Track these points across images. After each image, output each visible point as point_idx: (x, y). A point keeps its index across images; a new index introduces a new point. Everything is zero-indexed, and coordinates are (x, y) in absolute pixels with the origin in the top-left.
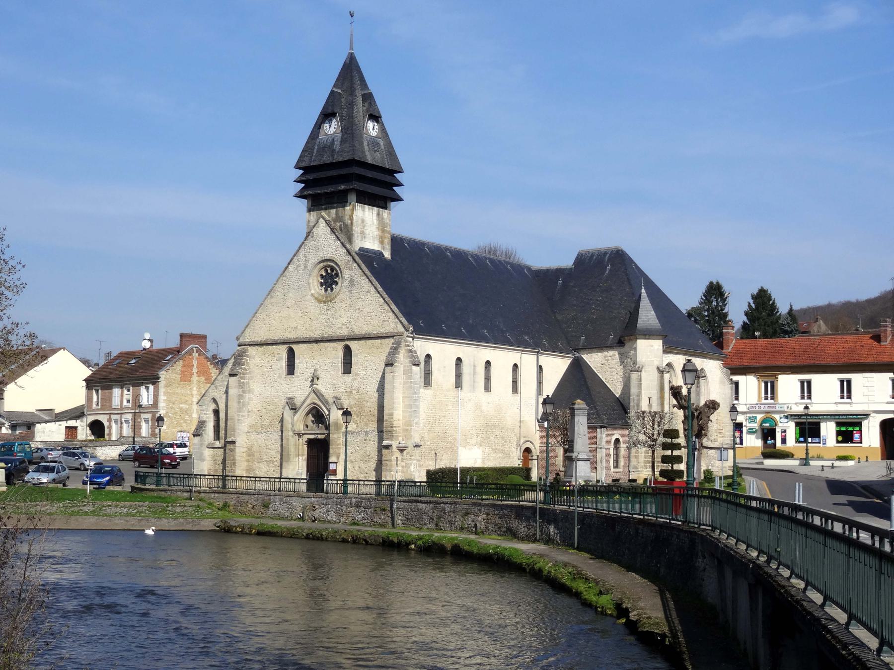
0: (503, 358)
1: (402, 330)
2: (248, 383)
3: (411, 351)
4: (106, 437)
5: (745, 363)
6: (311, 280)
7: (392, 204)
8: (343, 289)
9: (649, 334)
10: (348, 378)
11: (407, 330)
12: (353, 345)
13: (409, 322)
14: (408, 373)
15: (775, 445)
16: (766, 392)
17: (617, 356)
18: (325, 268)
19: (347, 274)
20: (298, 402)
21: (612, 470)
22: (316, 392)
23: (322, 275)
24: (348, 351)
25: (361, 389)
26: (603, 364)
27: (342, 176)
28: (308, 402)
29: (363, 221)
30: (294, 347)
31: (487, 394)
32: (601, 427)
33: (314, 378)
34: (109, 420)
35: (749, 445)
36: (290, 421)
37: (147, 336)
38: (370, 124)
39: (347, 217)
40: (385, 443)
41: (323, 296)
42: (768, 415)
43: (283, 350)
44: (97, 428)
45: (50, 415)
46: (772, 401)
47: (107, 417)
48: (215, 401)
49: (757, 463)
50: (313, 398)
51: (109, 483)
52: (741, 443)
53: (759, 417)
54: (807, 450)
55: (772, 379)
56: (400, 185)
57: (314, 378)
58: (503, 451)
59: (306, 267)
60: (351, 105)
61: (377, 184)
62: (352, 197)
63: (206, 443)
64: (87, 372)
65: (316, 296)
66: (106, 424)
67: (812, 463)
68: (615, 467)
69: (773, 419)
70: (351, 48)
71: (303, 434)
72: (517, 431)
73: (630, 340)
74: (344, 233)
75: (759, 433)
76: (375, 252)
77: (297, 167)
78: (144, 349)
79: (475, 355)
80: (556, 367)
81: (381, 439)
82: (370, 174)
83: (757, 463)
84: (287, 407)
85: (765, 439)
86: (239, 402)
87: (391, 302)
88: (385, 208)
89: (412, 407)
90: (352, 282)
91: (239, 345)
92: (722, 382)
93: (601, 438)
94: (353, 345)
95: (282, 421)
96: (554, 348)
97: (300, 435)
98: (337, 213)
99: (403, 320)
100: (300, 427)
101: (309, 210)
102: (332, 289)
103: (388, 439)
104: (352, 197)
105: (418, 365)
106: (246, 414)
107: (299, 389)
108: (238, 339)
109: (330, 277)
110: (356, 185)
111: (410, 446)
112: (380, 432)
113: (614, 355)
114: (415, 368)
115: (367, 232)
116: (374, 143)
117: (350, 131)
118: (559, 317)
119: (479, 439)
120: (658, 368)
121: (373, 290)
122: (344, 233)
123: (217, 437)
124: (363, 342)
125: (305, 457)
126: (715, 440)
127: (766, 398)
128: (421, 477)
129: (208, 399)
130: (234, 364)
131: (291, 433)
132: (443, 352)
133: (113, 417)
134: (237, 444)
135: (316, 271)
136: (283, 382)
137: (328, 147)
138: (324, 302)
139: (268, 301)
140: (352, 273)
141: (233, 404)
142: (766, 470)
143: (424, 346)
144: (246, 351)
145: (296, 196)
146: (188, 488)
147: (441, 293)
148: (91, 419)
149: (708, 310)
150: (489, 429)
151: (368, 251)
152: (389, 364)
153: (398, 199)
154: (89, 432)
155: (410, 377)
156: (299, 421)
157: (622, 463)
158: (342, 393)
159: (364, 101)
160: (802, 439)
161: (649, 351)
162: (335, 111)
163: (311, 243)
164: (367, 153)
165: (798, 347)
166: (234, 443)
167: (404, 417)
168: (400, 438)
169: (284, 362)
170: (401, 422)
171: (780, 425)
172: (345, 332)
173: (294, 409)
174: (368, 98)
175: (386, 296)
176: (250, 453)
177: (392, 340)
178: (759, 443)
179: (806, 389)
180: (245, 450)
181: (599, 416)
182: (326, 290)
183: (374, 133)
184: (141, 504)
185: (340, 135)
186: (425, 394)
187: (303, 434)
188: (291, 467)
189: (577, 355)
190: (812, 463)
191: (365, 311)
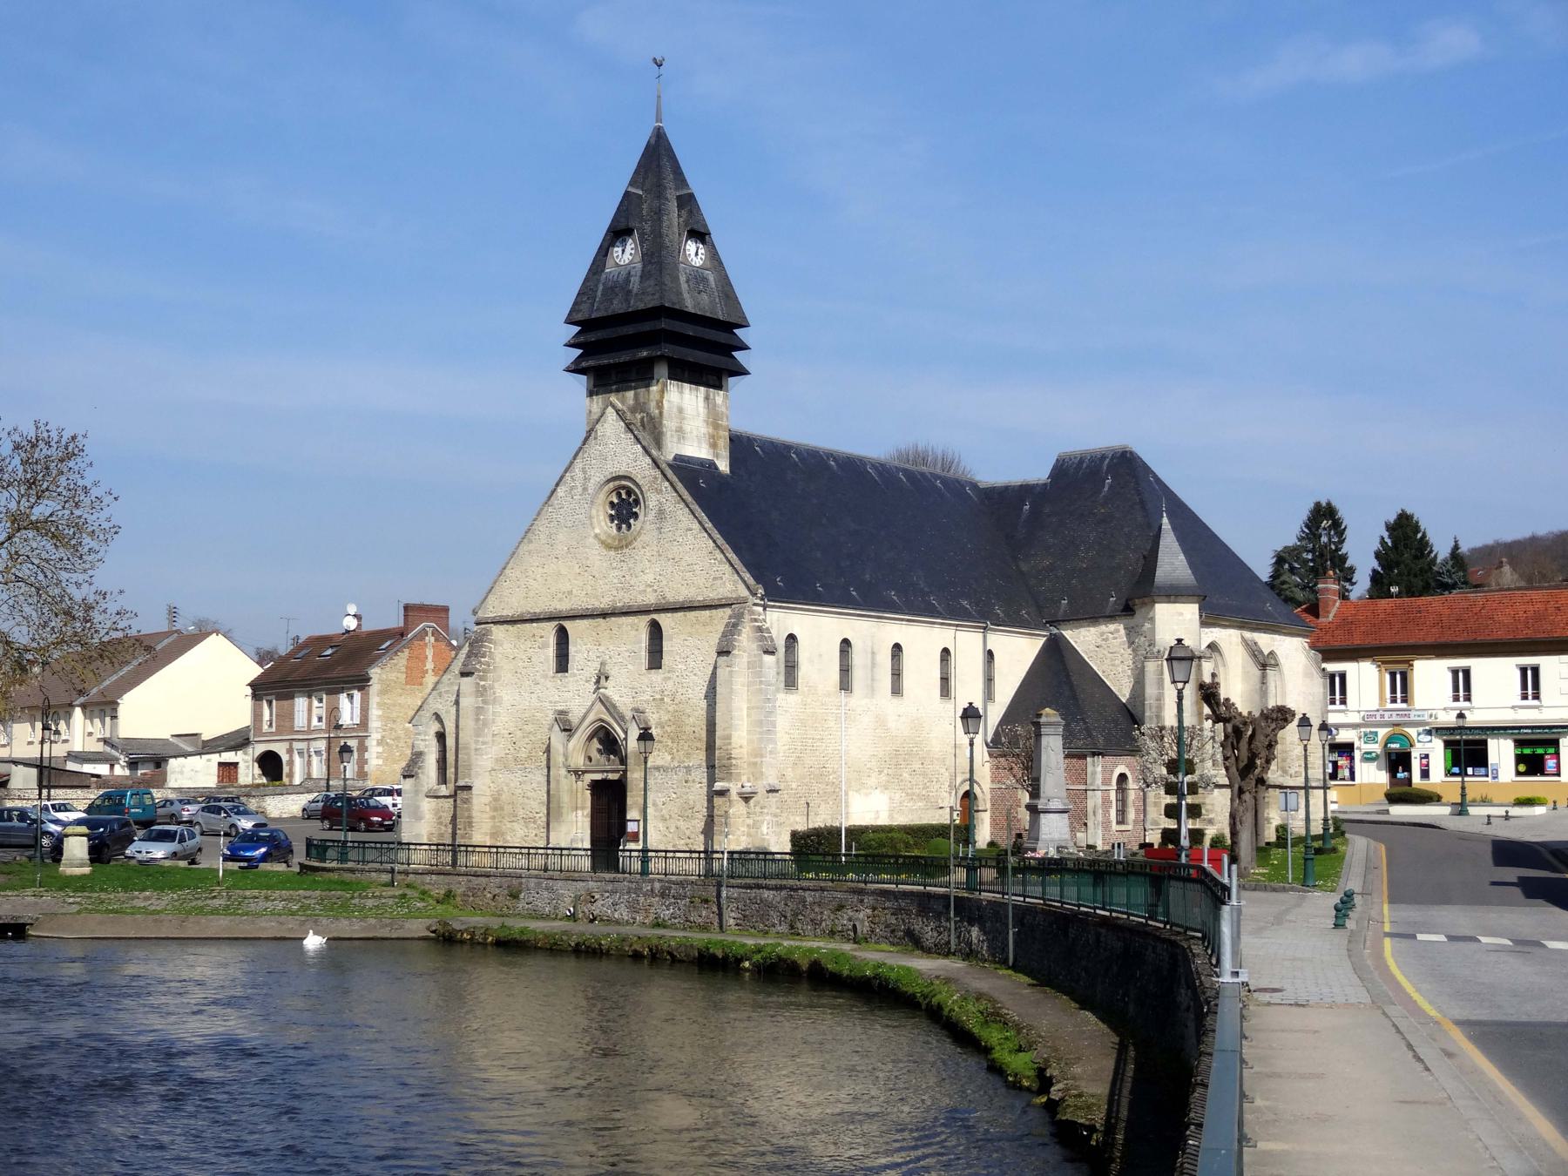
0: (922, 639)
1: (746, 593)
2: (492, 687)
3: (760, 629)
4: (285, 780)
5: (1357, 641)
6: (594, 512)
7: (731, 380)
8: (648, 526)
9: (1175, 594)
10: (656, 676)
11: (754, 595)
12: (664, 620)
13: (758, 579)
14: (755, 667)
15: (1409, 781)
16: (1393, 690)
17: (1123, 632)
18: (617, 490)
19: (652, 500)
20: (574, 718)
21: (1115, 827)
22: (604, 701)
23: (612, 503)
24: (656, 631)
25: (679, 696)
26: (1100, 646)
27: (645, 334)
28: (591, 717)
29: (681, 410)
30: (567, 624)
31: (896, 700)
32: (1094, 754)
33: (601, 677)
34: (290, 751)
35: (1365, 781)
36: (561, 750)
37: (352, 609)
38: (691, 247)
39: (653, 404)
40: (718, 786)
41: (614, 538)
42: (1397, 730)
43: (549, 631)
44: (271, 765)
45: (192, 744)
46: (1404, 706)
47: (286, 745)
48: (438, 717)
49: (1379, 812)
50: (599, 712)
51: (265, 858)
52: (1352, 777)
53: (1383, 732)
54: (1463, 788)
55: (1403, 667)
56: (744, 347)
57: (601, 677)
58: (926, 798)
59: (585, 489)
60: (658, 213)
61: (706, 347)
62: (662, 370)
63: (425, 789)
64: (255, 671)
65: (603, 537)
66: (285, 758)
67: (1472, 810)
68: (1118, 823)
69: (1407, 737)
70: (659, 119)
71: (584, 772)
72: (950, 761)
73: (1144, 604)
74: (648, 430)
75: (1383, 760)
76: (701, 462)
77: (570, 321)
78: (348, 631)
79: (873, 634)
80: (1018, 652)
81: (712, 780)
82: (690, 330)
83: (1379, 812)
84: (556, 728)
85: (1393, 771)
86: (478, 720)
87: (726, 547)
88: (719, 387)
89: (764, 725)
90: (661, 513)
91: (478, 624)
92: (1307, 675)
93: (1094, 773)
94: (664, 620)
95: (548, 750)
96: (1014, 621)
97: (578, 773)
98: (636, 397)
99: (747, 576)
100: (579, 761)
101: (591, 394)
102: (629, 527)
103: (722, 779)
104: (662, 370)
105: (772, 653)
106: (489, 739)
107: (575, 695)
108: (475, 612)
109: (625, 507)
110: (667, 350)
111: (762, 791)
112: (711, 767)
113: (1117, 631)
114: (768, 658)
115: (687, 428)
116: (697, 278)
117: (657, 258)
118: (1024, 567)
119: (883, 778)
121: (696, 526)
122: (648, 430)
123: (443, 779)
124: (680, 614)
125: (588, 811)
127: (1394, 701)
128: (780, 843)
129: (427, 714)
130: (468, 656)
131: (563, 772)
132: (817, 630)
133: (296, 745)
134: (474, 791)
135: (602, 496)
136: (549, 684)
137: (620, 287)
138: (616, 549)
139: (524, 547)
140: (661, 497)
141: (467, 723)
142: (1393, 823)
143: (782, 620)
144: (488, 632)
145: (568, 370)
146: (388, 866)
147: (816, 530)
148: (260, 749)
149: (1312, 551)
150: (900, 761)
151: (689, 460)
152: (723, 652)
153: (741, 371)
154: (257, 771)
155: (759, 674)
156: (576, 751)
157: (1131, 815)
158: (647, 702)
159: (680, 207)
160: (1456, 770)
161: (1175, 621)
162: (632, 224)
163: (593, 448)
164: (686, 295)
165: (1447, 612)
166: (469, 788)
167: (750, 741)
168: (744, 778)
169: (551, 651)
170: (744, 751)
171: (1418, 745)
172: (650, 599)
173: (568, 730)
174: (688, 202)
175: (717, 536)
176: (496, 805)
177: (728, 611)
178: (1381, 777)
179: (1463, 684)
180: (487, 800)
181: (1090, 735)
182: (619, 528)
183: (697, 262)
184: (308, 893)
185: (639, 266)
186: (787, 702)
187: (584, 772)
188: (564, 828)
190: (1472, 810)
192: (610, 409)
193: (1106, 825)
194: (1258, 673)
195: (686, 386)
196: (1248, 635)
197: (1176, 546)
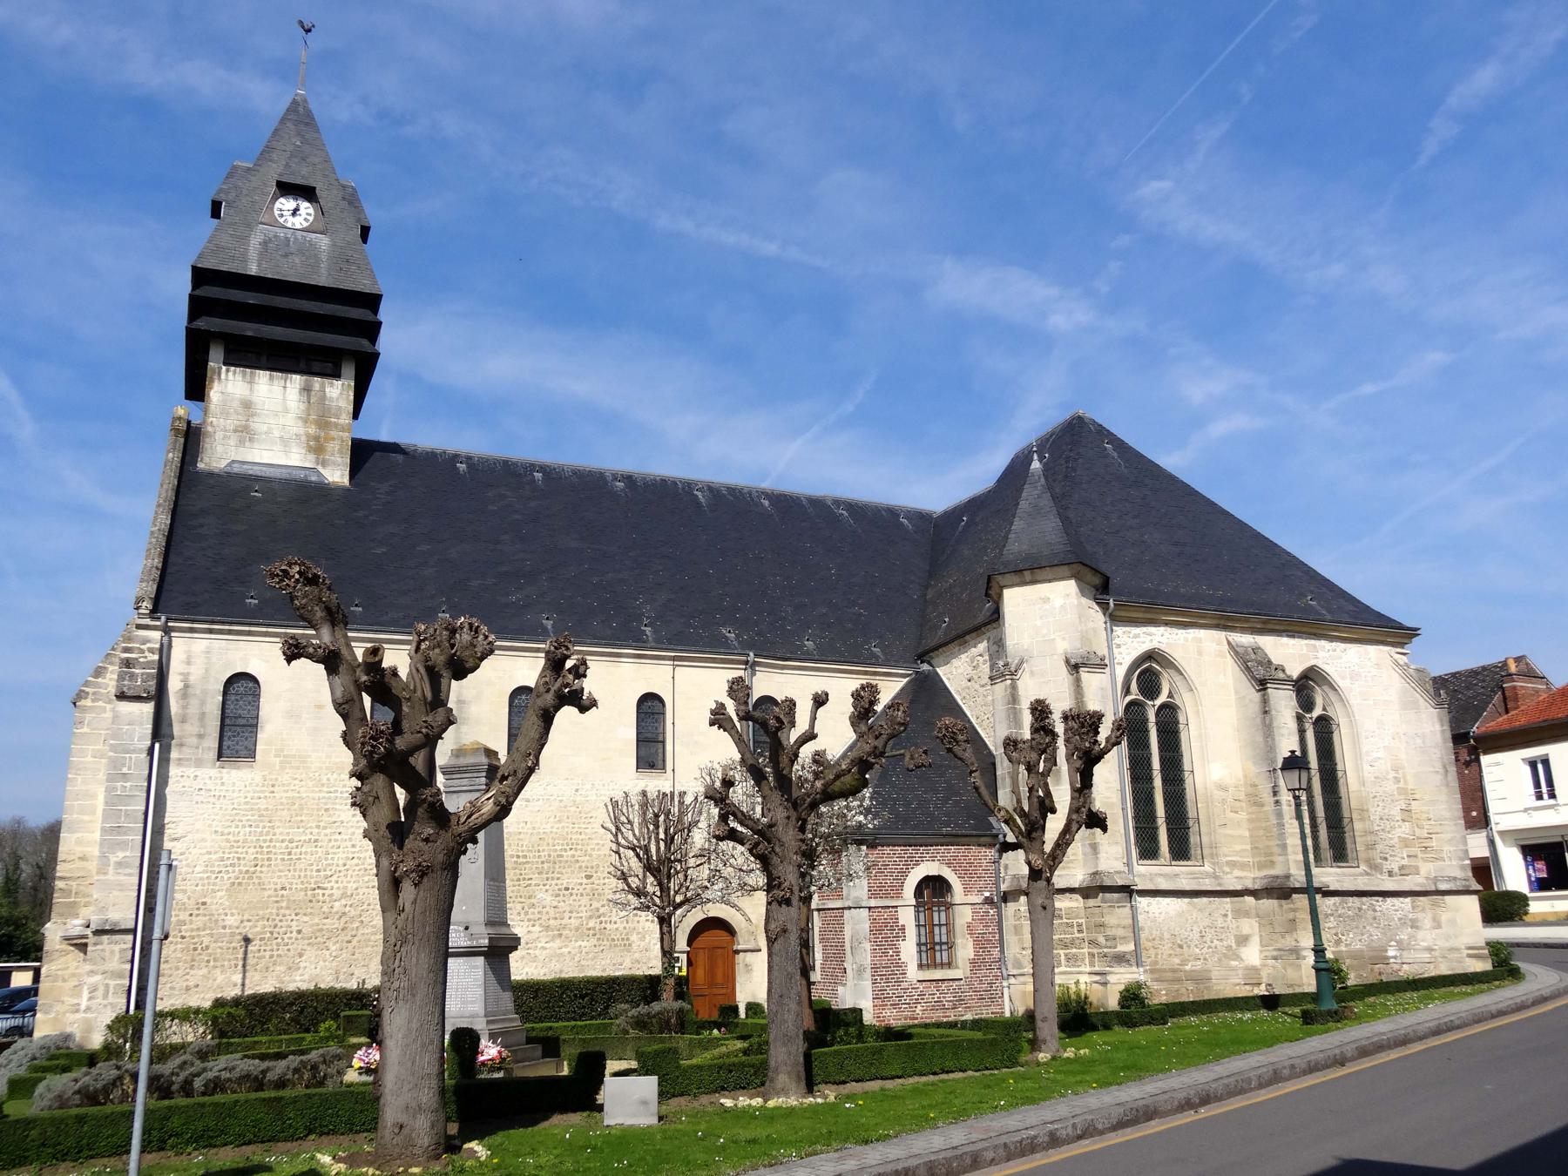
9: (1031, 570)
29: (247, 405)
38: (286, 204)
82: (251, 298)
92: (1406, 705)
120: (1067, 661)
126: (1404, 871)
183: (298, 222)
189: (925, 667)
193: (886, 971)
194: (1257, 696)
195: (262, 376)
196: (1244, 639)
197: (1046, 502)
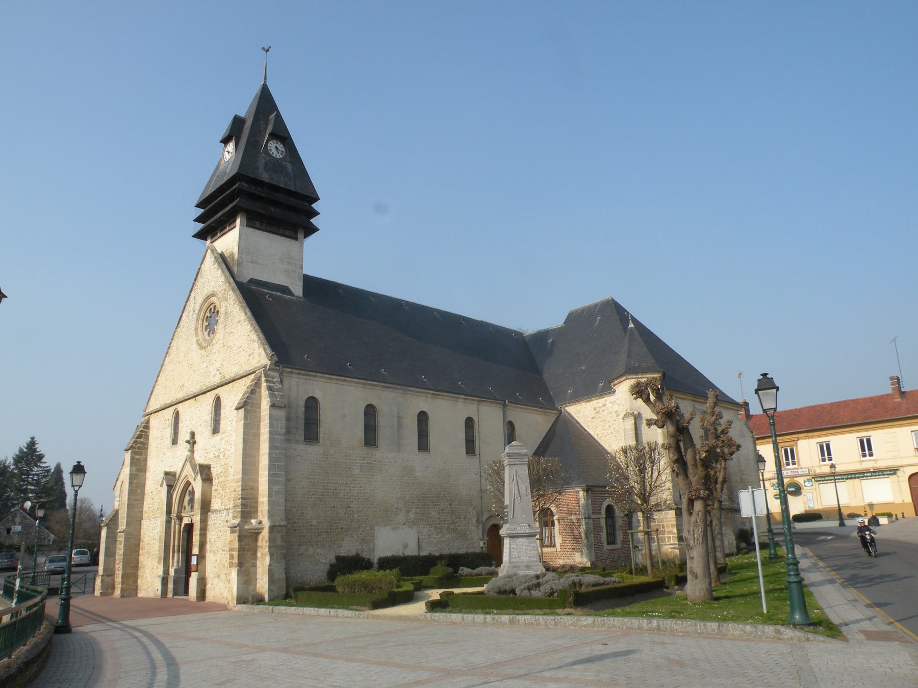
10: (217, 438)
21: (606, 547)
25: (227, 453)
31: (423, 455)
68: (609, 543)
116: (275, 165)
145: (194, 236)
157: (620, 537)
179: (825, 451)
191: (235, 348)
192: (209, 251)
